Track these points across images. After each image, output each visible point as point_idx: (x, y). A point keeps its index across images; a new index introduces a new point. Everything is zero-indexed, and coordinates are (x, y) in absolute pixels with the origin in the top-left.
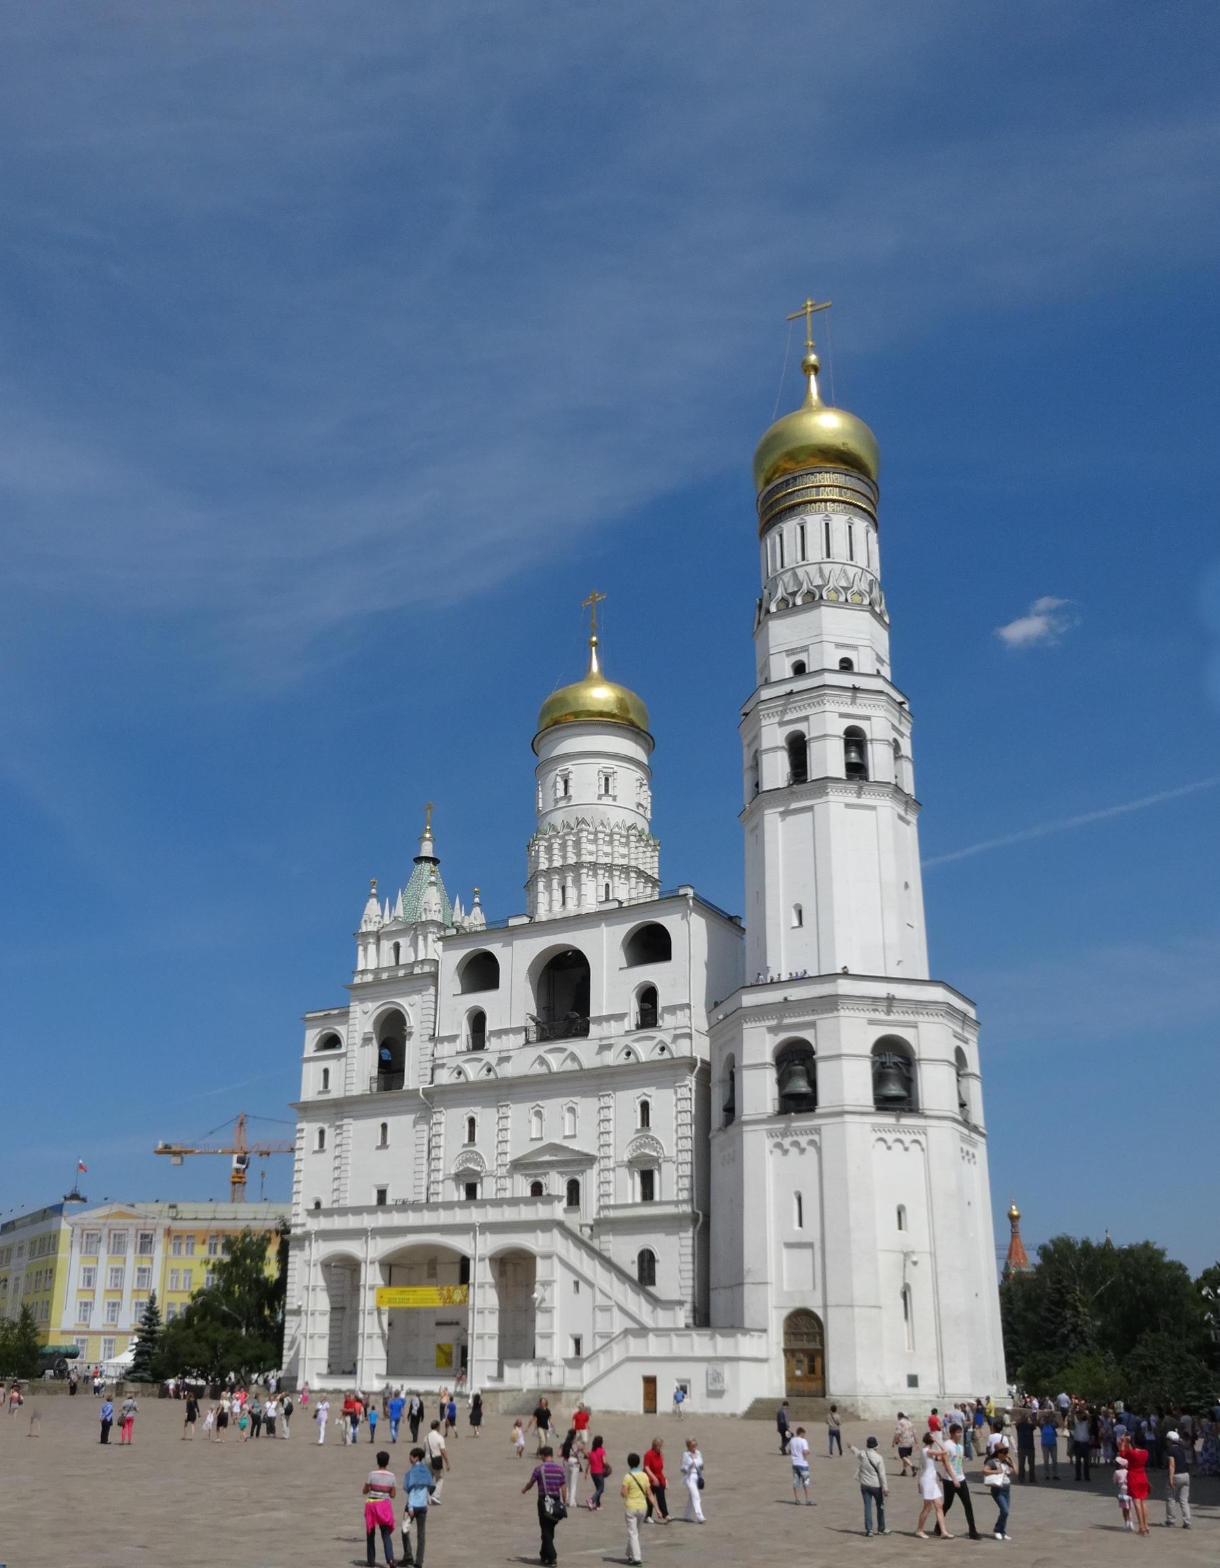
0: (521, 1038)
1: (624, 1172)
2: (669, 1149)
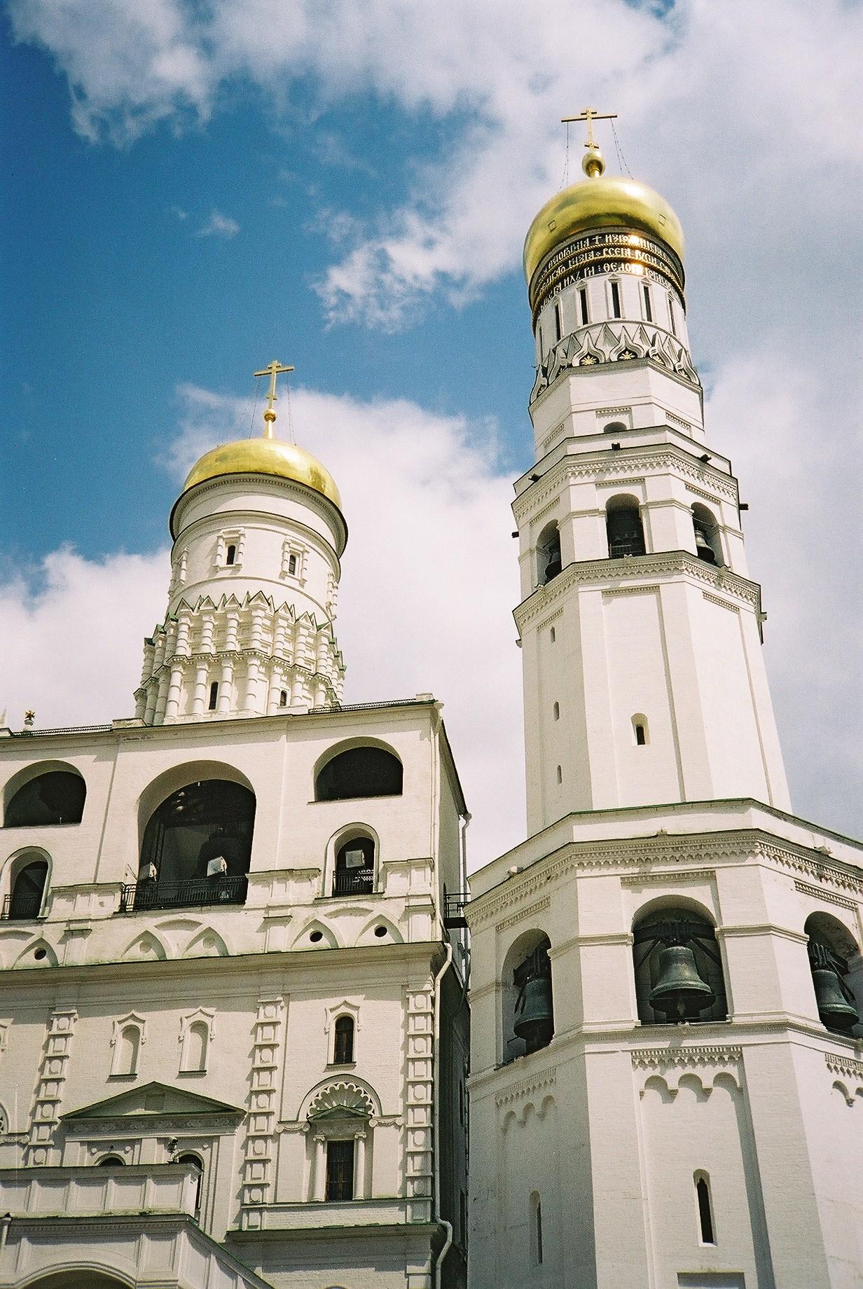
0: (112, 903)
1: (295, 1144)
2: (390, 1100)
